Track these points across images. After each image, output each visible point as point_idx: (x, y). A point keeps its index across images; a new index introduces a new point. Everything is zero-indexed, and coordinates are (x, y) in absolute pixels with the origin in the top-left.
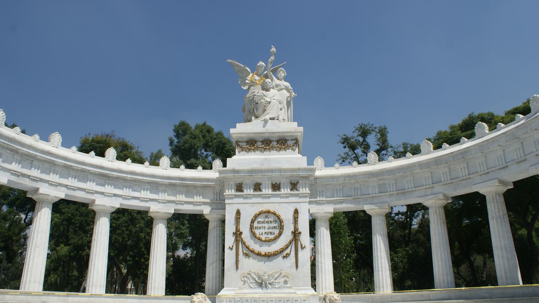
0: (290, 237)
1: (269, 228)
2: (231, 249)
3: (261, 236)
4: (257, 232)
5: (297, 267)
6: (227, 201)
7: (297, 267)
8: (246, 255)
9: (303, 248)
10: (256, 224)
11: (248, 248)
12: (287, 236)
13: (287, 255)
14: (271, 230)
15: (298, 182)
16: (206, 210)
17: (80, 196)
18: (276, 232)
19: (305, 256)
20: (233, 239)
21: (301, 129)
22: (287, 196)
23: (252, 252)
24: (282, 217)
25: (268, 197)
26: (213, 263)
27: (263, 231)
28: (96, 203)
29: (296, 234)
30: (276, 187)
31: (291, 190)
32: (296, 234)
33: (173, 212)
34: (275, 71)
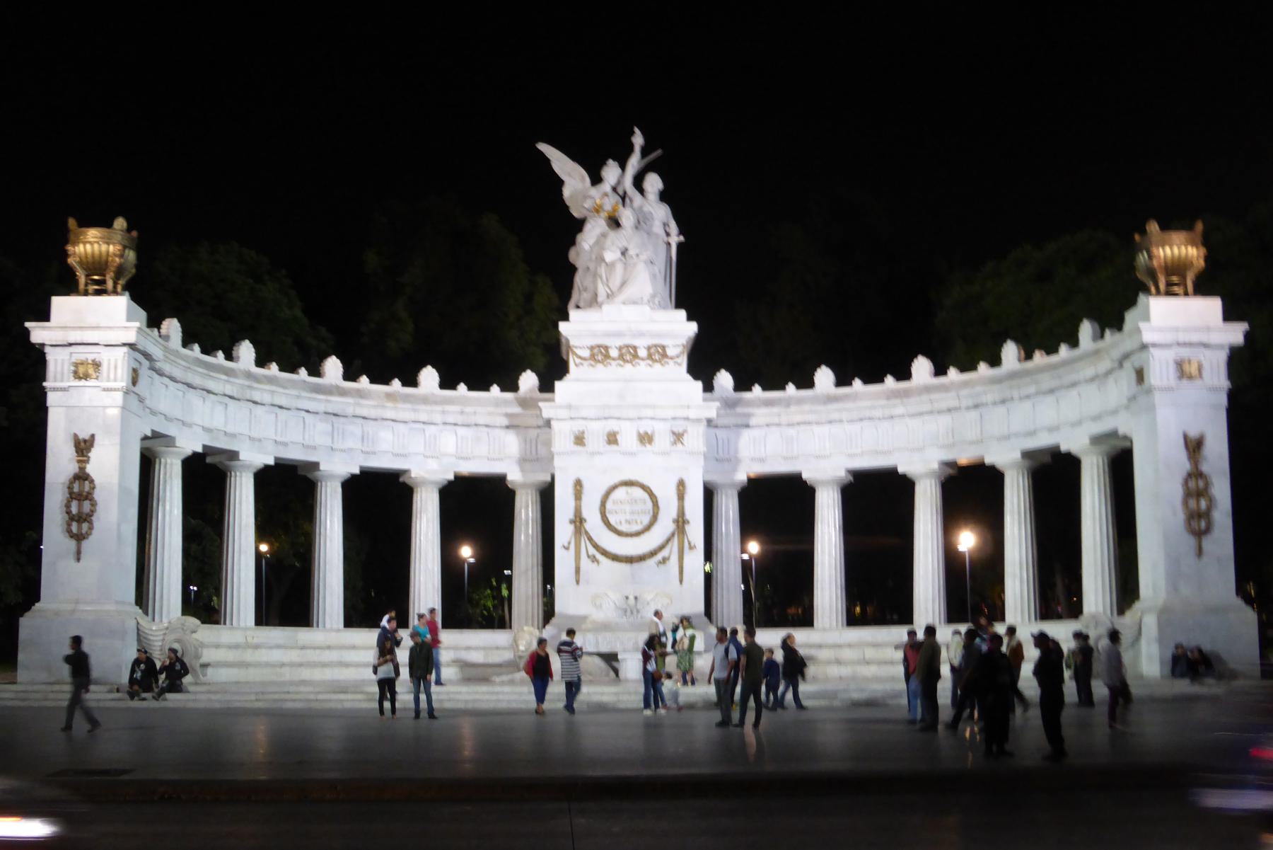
0: (671, 527)
1: (632, 513)
2: (567, 548)
3: (619, 528)
4: (613, 520)
5: (681, 581)
6: (558, 462)
7: (681, 581)
8: (594, 559)
9: (691, 548)
10: (609, 505)
11: (596, 546)
12: (665, 526)
13: (665, 561)
14: (635, 517)
15: (685, 431)
16: (514, 476)
17: (294, 454)
18: (646, 520)
19: (695, 563)
20: (571, 528)
21: (693, 328)
22: (665, 454)
23: (605, 553)
24: (655, 491)
25: (632, 454)
26: (527, 570)
27: (623, 518)
28: (322, 467)
29: (681, 522)
30: (646, 439)
31: (675, 443)
32: (681, 522)
33: (451, 477)
34: (638, 182)
